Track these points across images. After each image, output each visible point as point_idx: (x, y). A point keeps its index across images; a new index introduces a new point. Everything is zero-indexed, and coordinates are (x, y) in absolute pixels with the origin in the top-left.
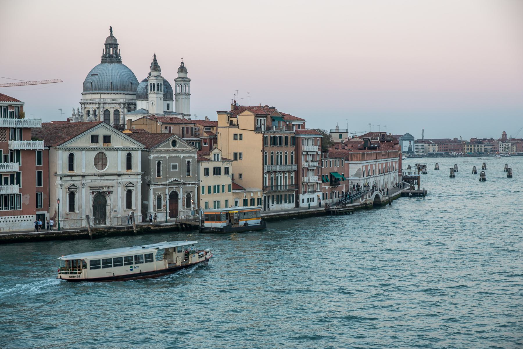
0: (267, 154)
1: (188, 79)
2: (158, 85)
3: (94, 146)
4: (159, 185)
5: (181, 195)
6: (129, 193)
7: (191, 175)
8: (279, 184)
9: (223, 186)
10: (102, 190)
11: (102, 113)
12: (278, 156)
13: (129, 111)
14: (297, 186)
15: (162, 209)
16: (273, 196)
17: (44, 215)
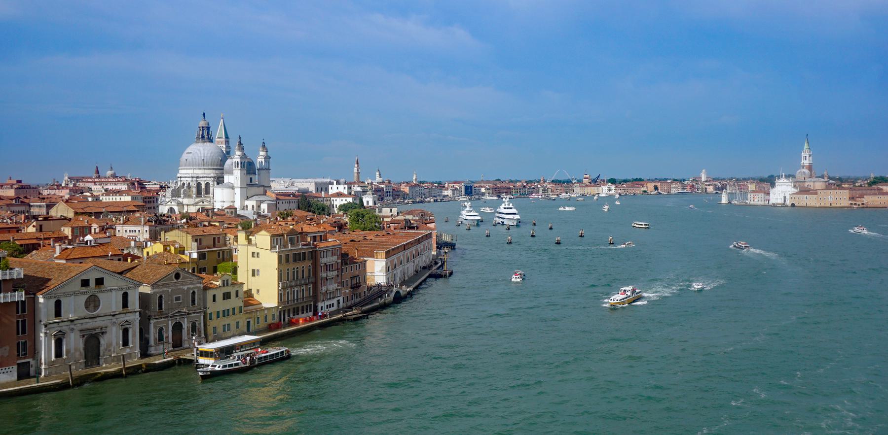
0: (283, 271)
1: (269, 156)
2: (241, 163)
3: (84, 289)
4: (161, 318)
5: (186, 325)
6: (126, 332)
7: (196, 304)
8: (296, 298)
9: (234, 309)
10: (94, 332)
11: (195, 186)
12: (294, 272)
13: (218, 184)
14: (315, 298)
15: (164, 341)
16: (289, 310)
17: (29, 362)
